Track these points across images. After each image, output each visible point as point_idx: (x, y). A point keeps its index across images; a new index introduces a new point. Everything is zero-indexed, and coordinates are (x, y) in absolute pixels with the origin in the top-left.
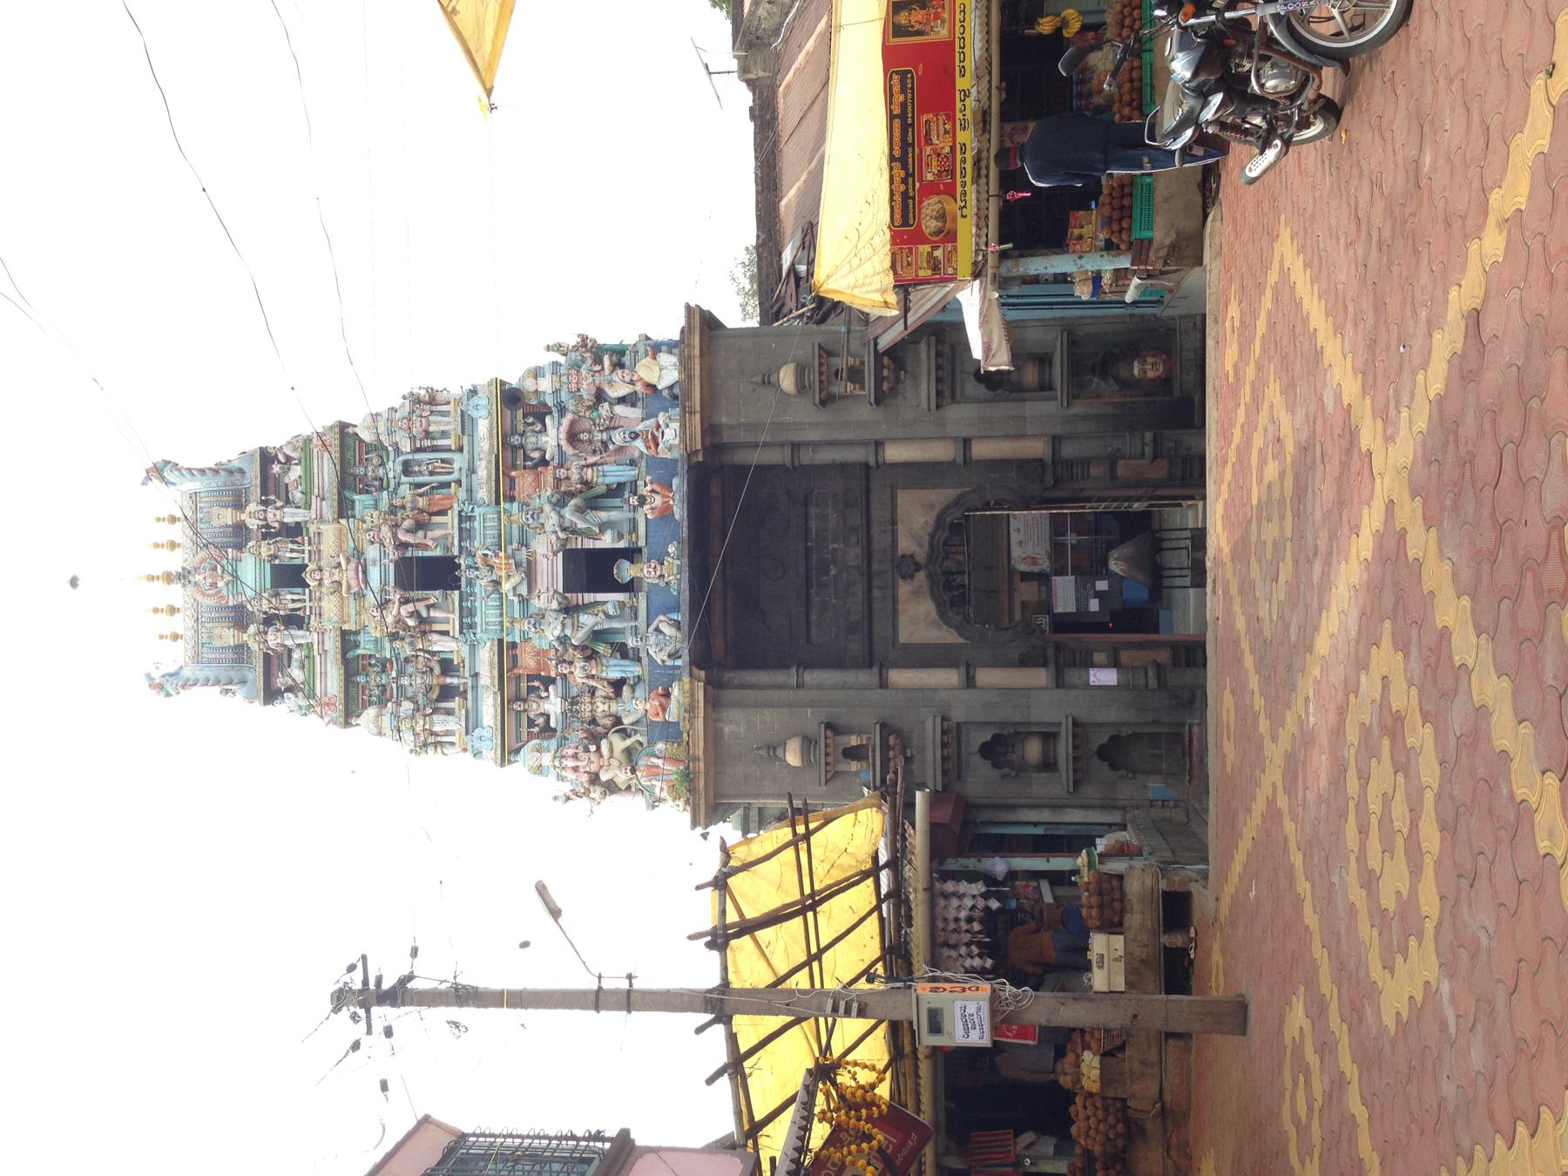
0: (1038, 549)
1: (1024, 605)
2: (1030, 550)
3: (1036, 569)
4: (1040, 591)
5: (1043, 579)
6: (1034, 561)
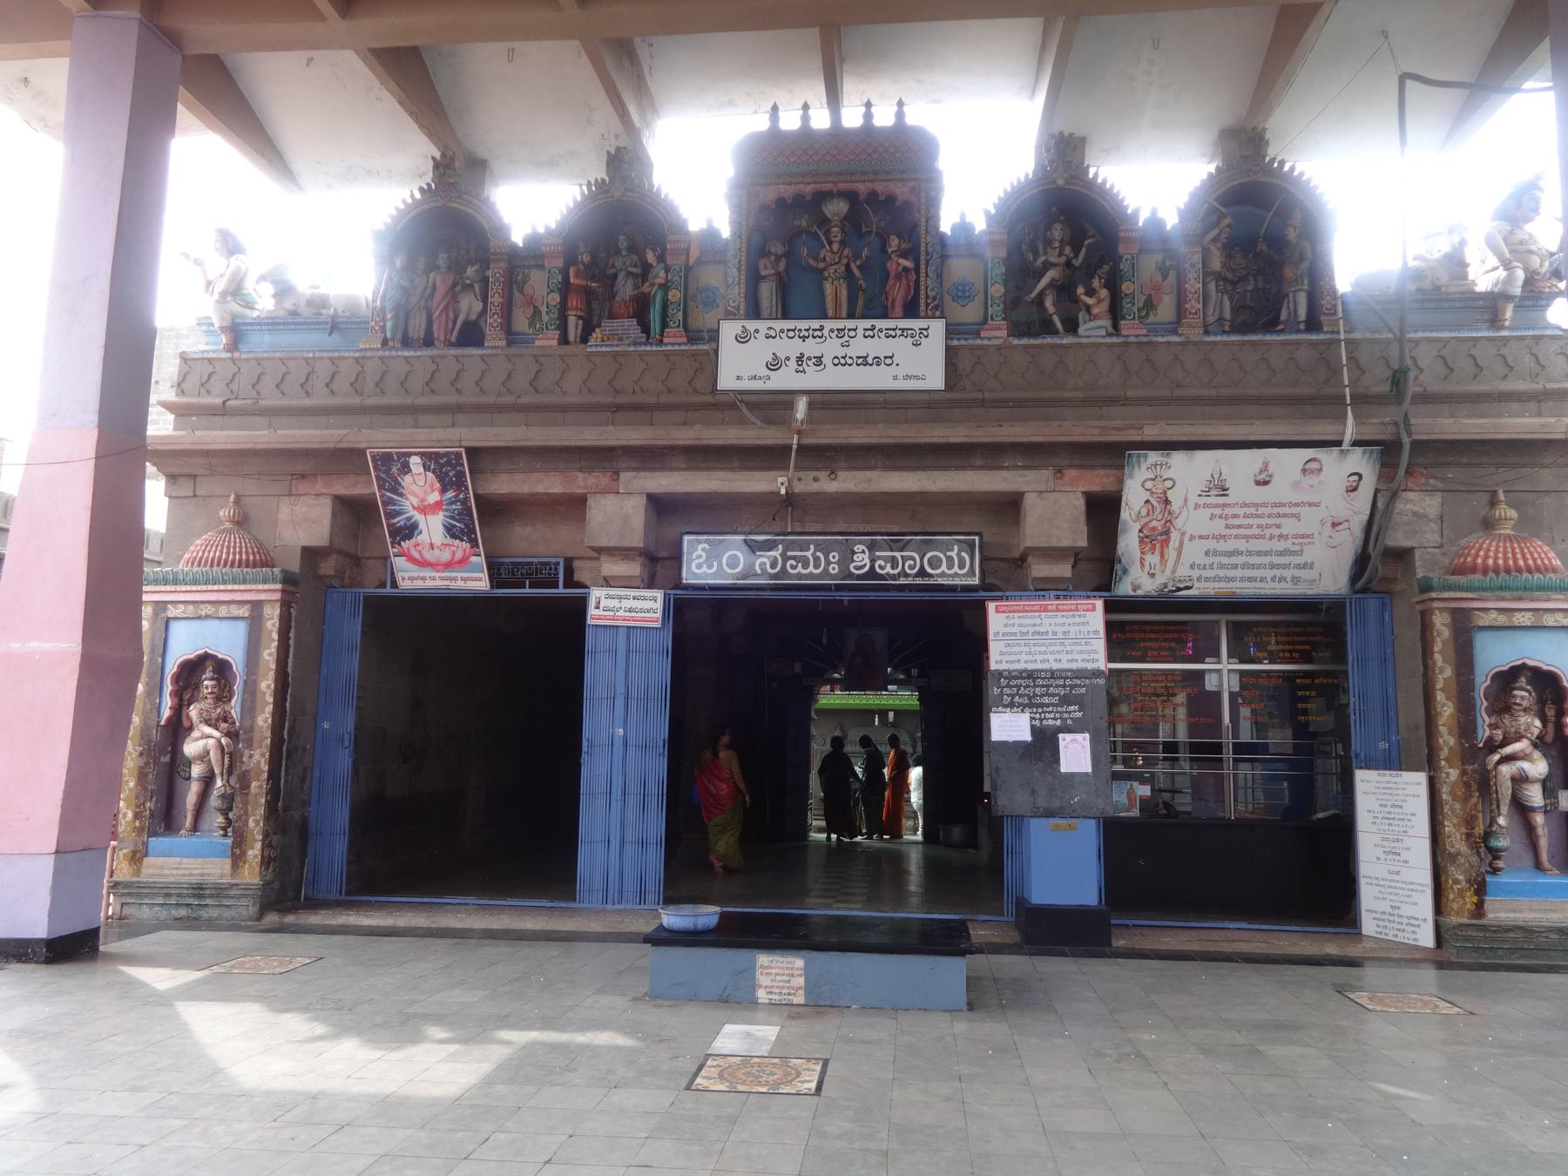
0: (1194, 552)
1: (1009, 507)
2: (1193, 521)
3: (1128, 542)
4: (1053, 554)
5: (1096, 566)
6: (1156, 539)
